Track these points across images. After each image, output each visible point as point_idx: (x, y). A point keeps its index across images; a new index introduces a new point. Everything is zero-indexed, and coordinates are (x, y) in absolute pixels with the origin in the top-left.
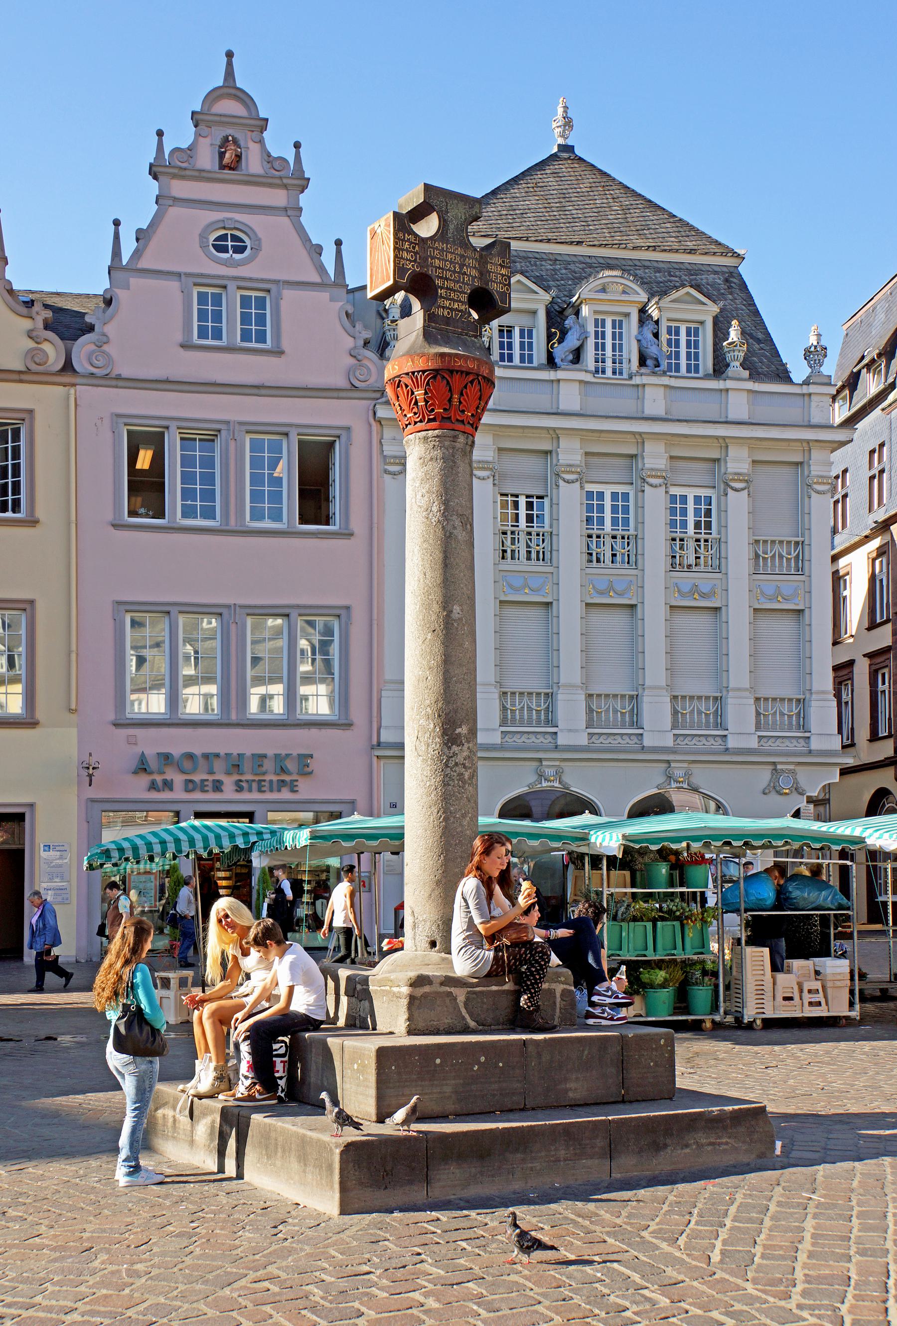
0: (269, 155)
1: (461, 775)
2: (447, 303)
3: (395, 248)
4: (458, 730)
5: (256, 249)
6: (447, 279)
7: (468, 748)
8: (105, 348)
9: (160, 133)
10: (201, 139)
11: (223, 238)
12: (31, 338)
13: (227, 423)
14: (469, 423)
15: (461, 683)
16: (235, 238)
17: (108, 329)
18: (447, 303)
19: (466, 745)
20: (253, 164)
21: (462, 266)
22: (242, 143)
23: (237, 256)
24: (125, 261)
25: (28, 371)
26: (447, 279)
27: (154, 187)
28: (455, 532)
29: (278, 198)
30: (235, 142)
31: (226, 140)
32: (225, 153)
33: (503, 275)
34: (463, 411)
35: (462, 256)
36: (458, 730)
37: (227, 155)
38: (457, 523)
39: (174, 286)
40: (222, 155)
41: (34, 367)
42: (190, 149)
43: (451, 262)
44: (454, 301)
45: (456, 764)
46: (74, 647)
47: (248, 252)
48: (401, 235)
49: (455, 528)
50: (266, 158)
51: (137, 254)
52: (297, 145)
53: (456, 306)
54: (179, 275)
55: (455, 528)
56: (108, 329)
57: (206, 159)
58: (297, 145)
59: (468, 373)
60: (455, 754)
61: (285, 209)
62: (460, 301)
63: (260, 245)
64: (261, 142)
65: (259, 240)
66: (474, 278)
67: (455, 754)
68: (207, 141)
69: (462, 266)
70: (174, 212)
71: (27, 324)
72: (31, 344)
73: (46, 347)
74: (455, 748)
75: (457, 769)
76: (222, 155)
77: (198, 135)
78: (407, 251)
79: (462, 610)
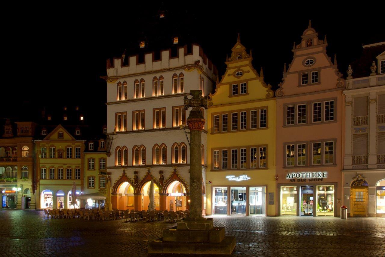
11: (308, 61)
16: (311, 60)
40: (307, 43)
48: (185, 100)
59: (195, 121)
71: (267, 89)
76: (307, 43)
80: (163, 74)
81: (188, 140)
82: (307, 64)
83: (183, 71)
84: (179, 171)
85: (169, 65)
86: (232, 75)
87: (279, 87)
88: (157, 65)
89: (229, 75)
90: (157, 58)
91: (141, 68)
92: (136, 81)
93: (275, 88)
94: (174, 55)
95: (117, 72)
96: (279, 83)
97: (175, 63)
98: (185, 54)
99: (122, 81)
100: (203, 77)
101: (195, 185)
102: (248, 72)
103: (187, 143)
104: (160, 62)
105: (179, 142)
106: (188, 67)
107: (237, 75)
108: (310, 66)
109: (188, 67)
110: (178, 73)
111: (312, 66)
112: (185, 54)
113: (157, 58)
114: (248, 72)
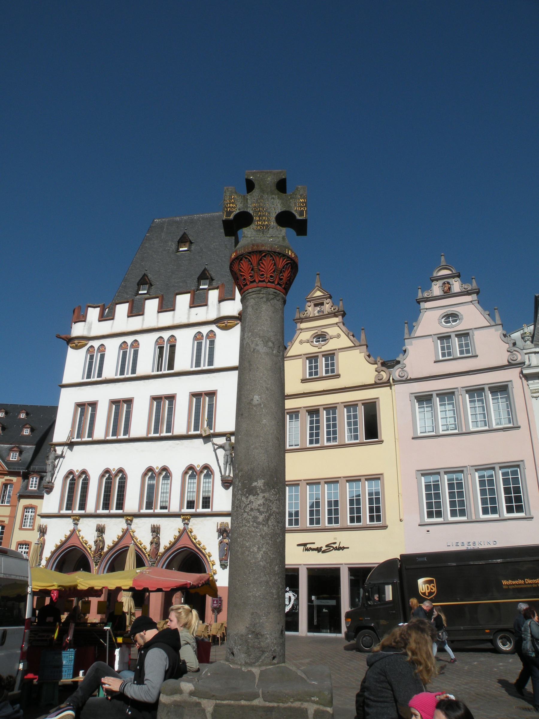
1: (255, 518)
4: (255, 484)
7: (264, 497)
15: (257, 449)
17: (405, 362)
19: (261, 495)
23: (454, 324)
25: (376, 384)
28: (257, 348)
30: (448, 283)
31: (444, 283)
36: (255, 484)
38: (260, 342)
39: (430, 339)
41: (378, 382)
45: (252, 510)
49: (257, 345)
54: (431, 335)
56: (405, 362)
60: (251, 502)
61: (471, 302)
67: (251, 502)
72: (377, 373)
73: (382, 373)
74: (251, 498)
75: (252, 513)
79: (261, 398)
80: (175, 332)
81: (218, 460)
83: (213, 327)
86: (308, 342)
87: (398, 362)
88: (167, 319)
89: (301, 342)
90: (167, 306)
93: (389, 364)
95: (90, 329)
96: (398, 356)
98: (221, 300)
99: (96, 344)
101: (255, 505)
102: (338, 336)
104: (171, 313)
105: (198, 463)
108: (452, 327)
110: (205, 330)
111: (455, 326)
112: (221, 300)
114: (338, 336)
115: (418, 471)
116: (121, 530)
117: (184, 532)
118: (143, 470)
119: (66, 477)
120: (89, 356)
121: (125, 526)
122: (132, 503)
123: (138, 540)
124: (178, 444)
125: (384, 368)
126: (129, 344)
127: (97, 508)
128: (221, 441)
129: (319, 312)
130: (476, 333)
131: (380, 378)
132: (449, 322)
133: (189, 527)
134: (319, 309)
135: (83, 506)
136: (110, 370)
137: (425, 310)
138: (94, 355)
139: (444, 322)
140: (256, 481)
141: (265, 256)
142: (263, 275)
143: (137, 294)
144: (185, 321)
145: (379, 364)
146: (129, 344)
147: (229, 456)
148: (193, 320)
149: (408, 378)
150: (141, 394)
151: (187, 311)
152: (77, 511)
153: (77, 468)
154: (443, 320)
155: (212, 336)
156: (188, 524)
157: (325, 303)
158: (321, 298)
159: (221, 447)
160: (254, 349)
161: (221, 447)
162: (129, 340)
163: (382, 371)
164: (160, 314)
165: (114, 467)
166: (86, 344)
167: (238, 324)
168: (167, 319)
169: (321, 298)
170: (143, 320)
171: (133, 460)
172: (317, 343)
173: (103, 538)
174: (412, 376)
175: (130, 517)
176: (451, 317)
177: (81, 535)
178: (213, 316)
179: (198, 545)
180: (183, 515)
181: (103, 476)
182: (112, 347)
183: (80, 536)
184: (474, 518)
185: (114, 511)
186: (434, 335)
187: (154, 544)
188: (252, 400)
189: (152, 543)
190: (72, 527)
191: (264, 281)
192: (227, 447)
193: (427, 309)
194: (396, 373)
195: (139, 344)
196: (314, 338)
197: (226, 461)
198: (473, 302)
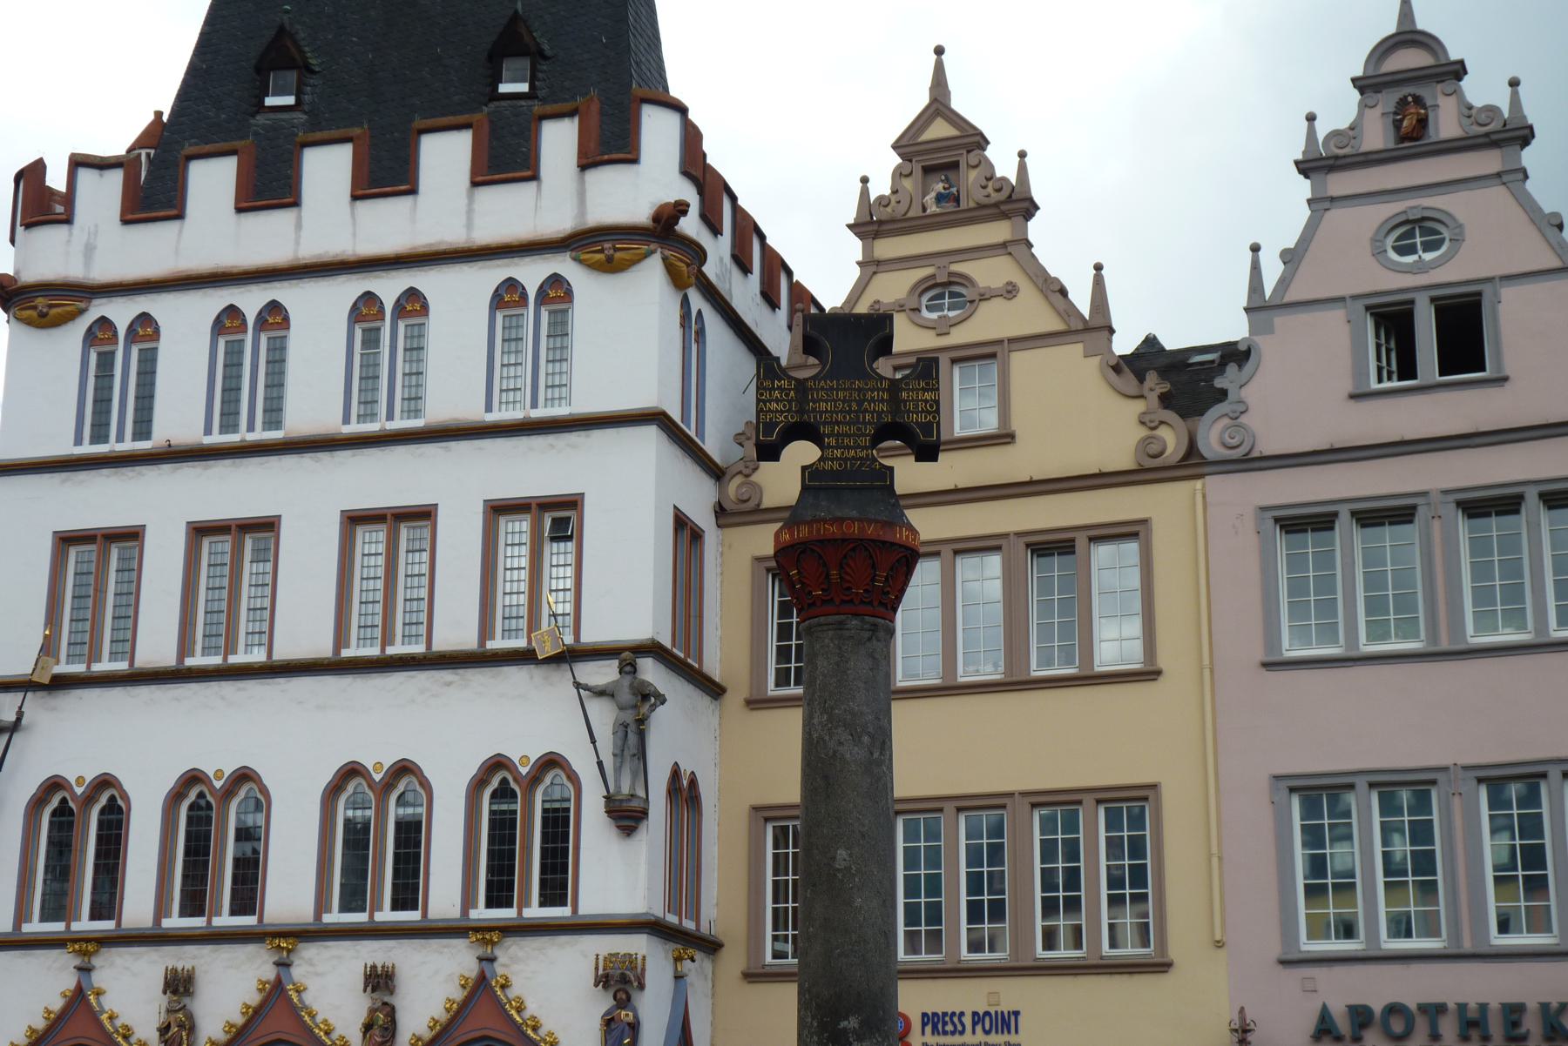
0: (1470, 107)
2: (838, 453)
3: (758, 401)
4: (844, 1024)
5: (1457, 241)
6: (837, 423)
8: (1244, 419)
9: (1311, 118)
10: (1367, 111)
12: (1143, 423)
13: (1424, 494)
14: (862, 602)
18: (838, 453)
20: (1446, 125)
21: (860, 404)
22: (1429, 102)
23: (1428, 256)
24: (1268, 292)
26: (837, 423)
27: (1304, 188)
29: (1489, 162)
30: (1418, 100)
31: (1403, 102)
32: (1401, 121)
33: (926, 401)
34: (849, 588)
35: (859, 390)
36: (844, 1024)
37: (1405, 123)
38: (845, 736)
39: (1337, 316)
40: (1397, 125)
42: (1352, 128)
43: (844, 401)
44: (849, 448)
46: (1215, 850)
47: (1444, 248)
48: (767, 383)
49: (841, 743)
50: (1466, 112)
51: (1284, 283)
52: (1514, 83)
53: (852, 453)
54: (1342, 299)
55: (841, 743)
57: (1377, 137)
58: (1514, 83)
62: (859, 446)
63: (1462, 233)
64: (1458, 93)
65: (1460, 226)
66: (880, 414)
68: (1378, 111)
69: (860, 404)
70: (1336, 215)
71: (1139, 406)
73: (1164, 432)
77: (1363, 106)
78: (777, 401)
79: (850, 855)
80: (427, 281)
81: (593, 742)
82: (1401, 251)
83: (564, 265)
84: (515, 968)
85: (469, 225)
87: (1223, 395)
88: (388, 225)
90: (386, 174)
91: (269, 238)
92: (229, 320)
94: (505, 160)
95: (89, 250)
97: (510, 212)
98: (587, 163)
99: (122, 312)
100: (700, 312)
102: (1010, 291)
103: (583, 763)
104: (403, 203)
105: (524, 750)
106: (605, 247)
107: (929, 308)
108: (1421, 268)
109: (605, 247)
110: (531, 273)
112: (587, 163)
113: (386, 174)
114: (1010, 291)
115: (1277, 778)
116: (254, 984)
117: (482, 990)
118: (327, 776)
119: (37, 803)
120: (93, 357)
121: (270, 973)
122: (290, 889)
123: (319, 1019)
124: (449, 684)
125: (1170, 415)
126: (251, 320)
127: (161, 910)
128: (603, 673)
129: (940, 198)
130: (1508, 293)
131: (1154, 449)
132: (1411, 250)
133: (499, 969)
134: (939, 187)
135: (107, 904)
136: (181, 413)
137: (1327, 204)
138: (113, 353)
139: (1396, 249)
140: (846, 1018)
141: (853, 549)
142: (849, 588)
143: (261, 107)
144: (452, 234)
145: (1153, 398)
146: (251, 320)
147: (632, 727)
148: (487, 233)
149: (1255, 454)
150: (308, 503)
151: (464, 201)
152: (84, 924)
153: (79, 769)
154: (1390, 241)
155: (556, 292)
156: (492, 960)
157: (963, 166)
158: (949, 148)
159: (600, 693)
160: (835, 752)
161: (600, 693)
162: (251, 301)
163: (1162, 423)
164: (362, 206)
165: (218, 763)
166: (82, 312)
167: (653, 252)
168: (388, 225)
169: (949, 148)
170: (299, 226)
171: (293, 745)
172: (934, 316)
173: (190, 1017)
174: (1269, 445)
175: (288, 939)
176: (1419, 231)
177: (107, 1008)
178: (559, 222)
179: (530, 1032)
180: (476, 930)
181: (175, 796)
182: (185, 324)
183: (103, 1011)
184: (1467, 946)
185: (225, 920)
186: (1355, 297)
187: (376, 1031)
188: (834, 858)
189: (368, 1027)
190: (69, 981)
191: (851, 601)
192: (626, 696)
193: (1332, 199)
194: (1213, 434)
195: (286, 319)
196: (921, 295)
197: (620, 743)
198: (1505, 178)
